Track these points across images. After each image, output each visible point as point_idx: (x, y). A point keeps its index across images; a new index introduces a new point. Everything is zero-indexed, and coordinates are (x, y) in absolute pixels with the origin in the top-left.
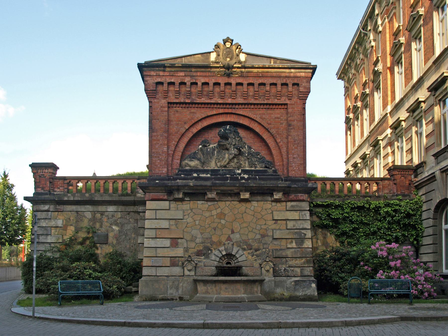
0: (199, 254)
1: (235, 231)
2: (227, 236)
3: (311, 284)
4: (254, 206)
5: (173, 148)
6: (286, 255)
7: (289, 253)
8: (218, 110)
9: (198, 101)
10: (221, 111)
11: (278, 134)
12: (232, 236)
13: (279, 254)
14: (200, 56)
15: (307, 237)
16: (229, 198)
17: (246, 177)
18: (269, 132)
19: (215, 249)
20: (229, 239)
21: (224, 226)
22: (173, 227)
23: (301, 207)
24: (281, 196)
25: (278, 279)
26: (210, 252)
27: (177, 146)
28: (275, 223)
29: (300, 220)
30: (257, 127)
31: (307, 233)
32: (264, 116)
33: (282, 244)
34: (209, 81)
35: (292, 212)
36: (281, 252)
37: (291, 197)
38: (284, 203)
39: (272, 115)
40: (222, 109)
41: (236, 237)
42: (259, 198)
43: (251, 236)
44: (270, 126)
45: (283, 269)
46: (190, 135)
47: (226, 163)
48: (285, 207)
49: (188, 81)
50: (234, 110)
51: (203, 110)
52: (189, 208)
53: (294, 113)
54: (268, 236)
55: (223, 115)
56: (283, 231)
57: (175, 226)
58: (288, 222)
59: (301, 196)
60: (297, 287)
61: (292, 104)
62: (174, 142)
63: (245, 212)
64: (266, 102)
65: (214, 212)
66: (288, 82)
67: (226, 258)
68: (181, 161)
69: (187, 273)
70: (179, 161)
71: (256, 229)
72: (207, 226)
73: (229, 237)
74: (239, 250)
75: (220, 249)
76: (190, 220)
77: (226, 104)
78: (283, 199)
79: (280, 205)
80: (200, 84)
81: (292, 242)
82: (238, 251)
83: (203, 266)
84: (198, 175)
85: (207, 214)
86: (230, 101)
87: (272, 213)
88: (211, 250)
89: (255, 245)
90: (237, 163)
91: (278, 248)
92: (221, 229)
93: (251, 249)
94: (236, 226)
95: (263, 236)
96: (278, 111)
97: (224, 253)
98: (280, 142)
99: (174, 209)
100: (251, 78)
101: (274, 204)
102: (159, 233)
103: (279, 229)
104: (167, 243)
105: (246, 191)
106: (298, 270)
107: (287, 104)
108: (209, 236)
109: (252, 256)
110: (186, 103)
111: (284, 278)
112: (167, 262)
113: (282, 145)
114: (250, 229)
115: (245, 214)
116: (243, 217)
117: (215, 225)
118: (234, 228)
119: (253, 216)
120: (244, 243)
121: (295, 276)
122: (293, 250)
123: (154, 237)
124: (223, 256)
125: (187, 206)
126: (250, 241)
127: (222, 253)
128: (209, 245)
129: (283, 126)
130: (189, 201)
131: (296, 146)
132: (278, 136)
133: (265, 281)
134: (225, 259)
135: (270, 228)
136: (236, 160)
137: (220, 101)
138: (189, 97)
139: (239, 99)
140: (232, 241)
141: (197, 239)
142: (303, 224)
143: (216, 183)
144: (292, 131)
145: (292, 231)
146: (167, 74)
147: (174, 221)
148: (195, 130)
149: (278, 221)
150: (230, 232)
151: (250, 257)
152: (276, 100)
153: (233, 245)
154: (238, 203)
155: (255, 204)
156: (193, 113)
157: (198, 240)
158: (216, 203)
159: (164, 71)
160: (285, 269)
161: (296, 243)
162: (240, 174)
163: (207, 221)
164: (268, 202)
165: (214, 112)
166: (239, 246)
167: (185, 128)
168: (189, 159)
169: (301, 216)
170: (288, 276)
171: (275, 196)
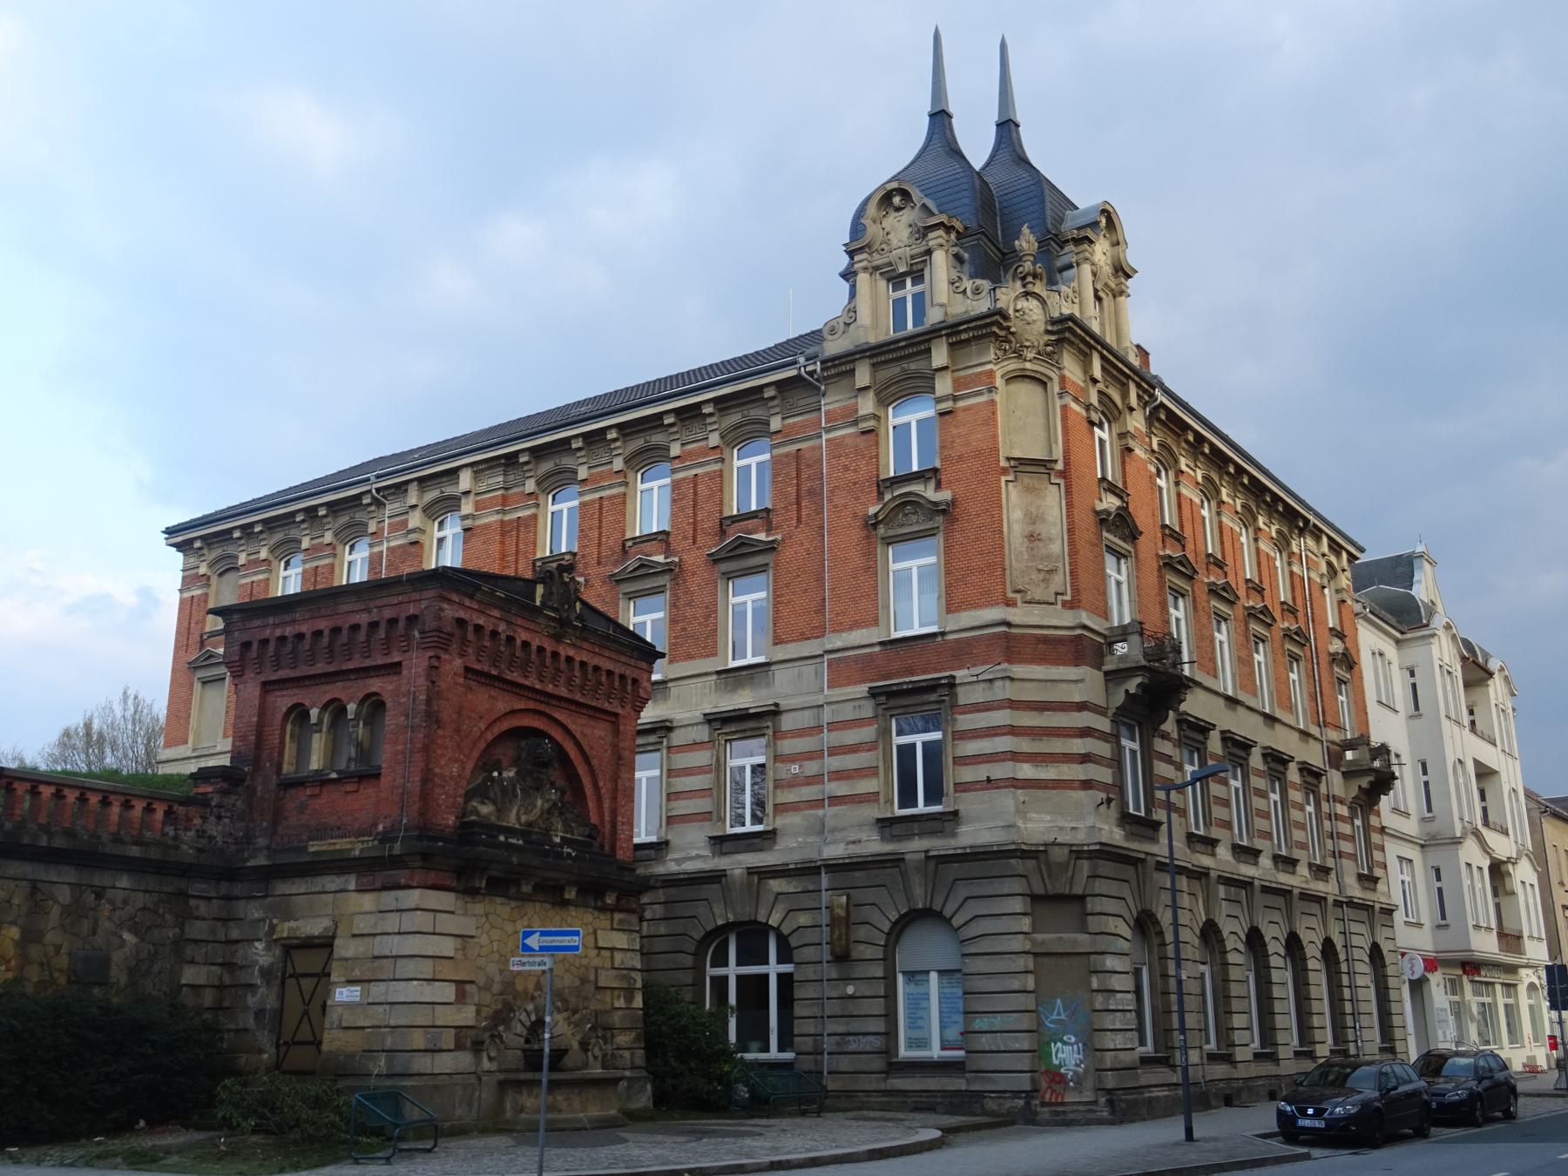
10: (532, 705)
69: (486, 1065)
76: (484, 940)
85: (509, 928)
87: (595, 932)
95: (584, 981)
106: (627, 1054)
112: (448, 1039)
128: (510, 998)
159: (471, 597)
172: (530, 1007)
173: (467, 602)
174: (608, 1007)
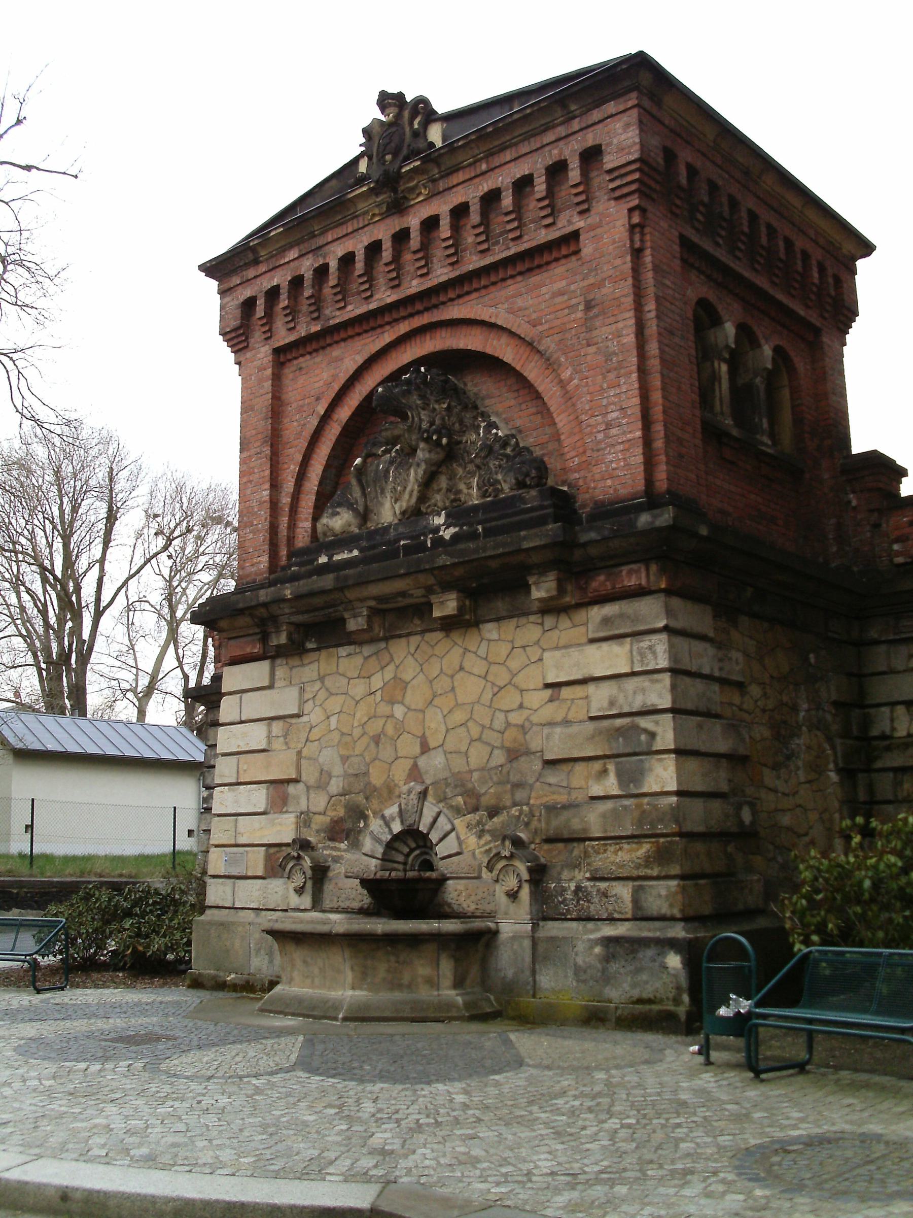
1: (432, 744)
2: (407, 764)
4: (489, 640)
6: (585, 830)
7: (593, 820)
10: (403, 328)
12: (422, 762)
13: (556, 824)
14: (334, 183)
15: (658, 745)
20: (415, 773)
22: (278, 744)
23: (636, 620)
25: (553, 929)
26: (362, 825)
27: (301, 477)
28: (551, 700)
29: (633, 674)
31: (659, 730)
32: (520, 302)
33: (575, 783)
35: (605, 646)
36: (565, 815)
37: (594, 584)
41: (434, 765)
43: (478, 756)
44: (540, 328)
45: (573, 886)
46: (333, 431)
50: (435, 311)
52: (315, 675)
56: (575, 729)
57: (282, 739)
59: (630, 573)
60: (614, 967)
61: (592, 228)
63: (461, 668)
65: (377, 682)
66: (566, 154)
67: (413, 845)
71: (490, 728)
72: (357, 732)
73: (415, 766)
74: (439, 814)
75: (388, 812)
81: (605, 771)
82: (435, 820)
85: (359, 689)
88: (365, 818)
89: (489, 793)
90: (449, 490)
92: (394, 740)
93: (476, 809)
95: (514, 754)
97: (397, 827)
98: (571, 379)
100: (460, 187)
101: (549, 621)
103: (566, 722)
104: (258, 798)
105: (446, 587)
106: (624, 892)
107: (575, 236)
108: (364, 769)
109: (480, 837)
111: (574, 924)
112: (256, 861)
114: (475, 731)
115: (462, 674)
116: (453, 689)
117: (375, 727)
118: (427, 734)
119: (485, 678)
120: (456, 786)
121: (611, 919)
122: (609, 805)
123: (234, 780)
124: (396, 838)
125: (309, 670)
126: (476, 775)
128: (360, 799)
130: (318, 649)
131: (611, 376)
134: (412, 850)
135: (535, 719)
141: (333, 781)
142: (643, 690)
145: (606, 723)
146: (262, 268)
150: (417, 750)
151: (472, 841)
152: (543, 231)
153: (423, 795)
159: (256, 262)
160: (578, 888)
161: (619, 775)
162: (437, 529)
163: (358, 715)
165: (388, 337)
166: (443, 799)
168: (330, 511)
169: (637, 657)
170: (589, 919)
171: (533, 588)
172: (392, 810)
173: (251, 273)
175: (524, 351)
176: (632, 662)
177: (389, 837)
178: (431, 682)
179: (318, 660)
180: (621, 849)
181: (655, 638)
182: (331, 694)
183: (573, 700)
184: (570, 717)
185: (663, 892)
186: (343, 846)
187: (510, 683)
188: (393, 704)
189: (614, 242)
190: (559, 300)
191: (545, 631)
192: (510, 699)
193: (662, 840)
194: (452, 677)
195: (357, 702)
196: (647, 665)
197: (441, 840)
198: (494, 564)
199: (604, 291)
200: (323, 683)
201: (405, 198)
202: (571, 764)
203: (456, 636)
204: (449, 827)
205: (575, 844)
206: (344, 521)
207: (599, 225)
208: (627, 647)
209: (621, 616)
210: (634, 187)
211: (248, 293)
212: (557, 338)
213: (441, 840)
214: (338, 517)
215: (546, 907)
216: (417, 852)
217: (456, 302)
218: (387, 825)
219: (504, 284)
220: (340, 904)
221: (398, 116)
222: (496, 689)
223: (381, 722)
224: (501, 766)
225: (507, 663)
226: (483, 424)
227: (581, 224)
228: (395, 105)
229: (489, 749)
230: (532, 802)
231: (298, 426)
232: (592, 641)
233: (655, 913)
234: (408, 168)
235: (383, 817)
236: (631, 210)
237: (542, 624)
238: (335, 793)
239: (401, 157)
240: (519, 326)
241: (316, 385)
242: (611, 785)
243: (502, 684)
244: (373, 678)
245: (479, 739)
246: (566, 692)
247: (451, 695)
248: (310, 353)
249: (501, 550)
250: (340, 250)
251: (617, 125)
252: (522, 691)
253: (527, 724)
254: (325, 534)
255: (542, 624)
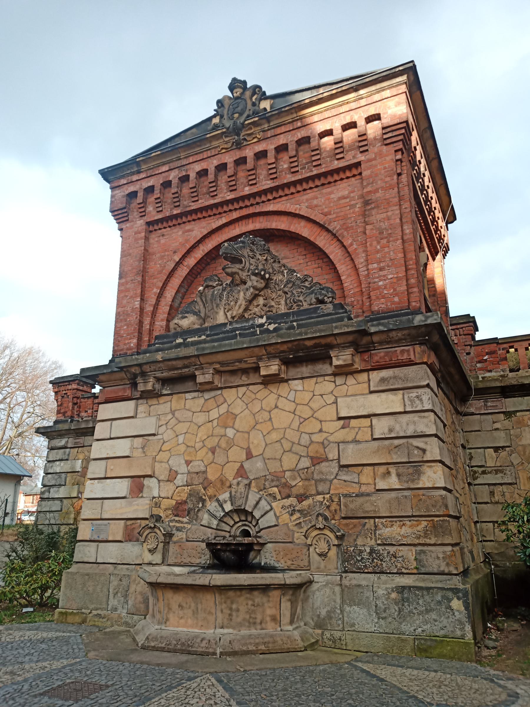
0: (179, 509)
1: (254, 453)
3: (450, 600)
4: (296, 391)
5: (154, 301)
7: (381, 504)
8: (230, 214)
9: (194, 206)
10: (235, 215)
11: (346, 229)
12: (246, 465)
14: (194, 130)
16: (244, 378)
17: (271, 329)
18: (328, 230)
19: (210, 498)
20: (241, 472)
21: (231, 443)
22: (138, 453)
24: (350, 357)
27: (160, 296)
28: (343, 427)
29: (405, 412)
30: (305, 227)
31: (428, 448)
32: (315, 202)
33: (364, 480)
34: (208, 165)
35: (383, 395)
36: (361, 500)
37: (376, 358)
38: (364, 376)
39: (332, 196)
40: (238, 212)
41: (256, 468)
42: (305, 370)
43: (289, 461)
45: (368, 550)
46: (183, 272)
47: (241, 311)
48: (366, 385)
49: (175, 177)
50: (257, 206)
51: (203, 223)
52: (168, 410)
53: (376, 175)
54: (327, 460)
55: (240, 223)
57: (141, 450)
58: (375, 420)
61: (370, 160)
62: (155, 290)
63: (276, 407)
64: (315, 172)
65: (214, 414)
67: (237, 520)
68: (168, 321)
70: (164, 323)
71: (299, 444)
72: (198, 445)
73: (242, 466)
74: (260, 499)
76: (168, 435)
77: (243, 198)
78: (357, 366)
79: (354, 382)
80: (192, 175)
81: (389, 473)
82: (258, 503)
83: (184, 540)
84: (185, 340)
85: (201, 418)
86: (247, 190)
87: (336, 402)
88: (204, 501)
90: (265, 305)
91: (354, 489)
93: (288, 496)
94: (257, 442)
96: (343, 185)
97: (228, 507)
98: (351, 244)
99: (143, 415)
100: (282, 136)
101: (339, 380)
102: (112, 467)
103: (355, 441)
104: (122, 487)
105: (271, 356)
106: (410, 553)
107: (358, 164)
108: (203, 469)
109: (292, 515)
110: (176, 217)
112: (117, 530)
113: (356, 249)
114: (287, 446)
115: (276, 410)
116: (270, 419)
119: (294, 413)
120: (273, 481)
122: (393, 494)
123: (103, 476)
124: (227, 514)
125: (163, 406)
126: (288, 474)
127: (225, 506)
129: (357, 210)
130: (171, 394)
131: (384, 241)
132: (345, 233)
133: (315, 586)
134: (236, 523)
135: (331, 439)
136: (261, 301)
137: (230, 196)
138: (178, 204)
139: (264, 183)
140: (248, 478)
141: (179, 476)
142: (414, 423)
143: (204, 349)
144: (374, 212)
147: (140, 439)
148: (191, 261)
149: (352, 421)
150: (244, 457)
151: (285, 517)
152: (336, 162)
153: (249, 485)
154: (261, 387)
155: (297, 385)
156: (189, 231)
157: (180, 480)
158: (219, 392)
159: (139, 172)
160: (372, 551)
161: (398, 475)
162: (262, 325)
163: (199, 435)
164: (327, 378)
165: (224, 220)
167: (174, 260)
168: (180, 316)
169: (407, 402)
171: (334, 359)
172: (225, 496)
173: (135, 178)
174: (371, 489)
175: (316, 229)
176: (405, 405)
177: (222, 514)
178: (254, 415)
179: (171, 401)
180: (404, 525)
181: (420, 391)
182: (180, 422)
183: (360, 428)
184: (358, 438)
185: (441, 556)
186: (185, 520)
187: (312, 416)
188: (226, 428)
189: (385, 168)
190: (343, 201)
191: (336, 386)
192: (313, 426)
193: (436, 519)
194: (270, 412)
195: (199, 427)
196: (416, 407)
197: (262, 516)
198: (309, 343)
199: (378, 195)
200: (174, 415)
201: (245, 139)
202: (361, 468)
203: (273, 388)
204: (269, 508)
205: (367, 521)
206: (190, 321)
207: (375, 159)
208: (400, 396)
209: (395, 377)
210: (401, 137)
211: (132, 188)
212: (341, 222)
213: (262, 516)
214: (186, 319)
215: (350, 563)
216: (240, 524)
217: (271, 202)
218: (221, 506)
219: (305, 192)
220: (183, 560)
221: (242, 94)
222: (302, 420)
223: (216, 440)
224: (307, 468)
225: (310, 404)
226: (285, 271)
227: (363, 158)
228: (241, 87)
229: (298, 457)
230: (331, 492)
231: (160, 266)
232: (371, 392)
233: (435, 571)
234: (250, 121)
235: (218, 500)
236: (396, 151)
237: (335, 382)
238: (181, 484)
239: (245, 115)
240: (315, 215)
241: (173, 245)
242: (393, 482)
243: (306, 417)
244: (211, 412)
245: (290, 451)
246: (353, 422)
247: (269, 423)
248: (170, 227)
249: (318, 334)
250: (198, 167)
251: (391, 103)
252: (321, 421)
253: (325, 442)
254: (175, 329)
255: (335, 382)
